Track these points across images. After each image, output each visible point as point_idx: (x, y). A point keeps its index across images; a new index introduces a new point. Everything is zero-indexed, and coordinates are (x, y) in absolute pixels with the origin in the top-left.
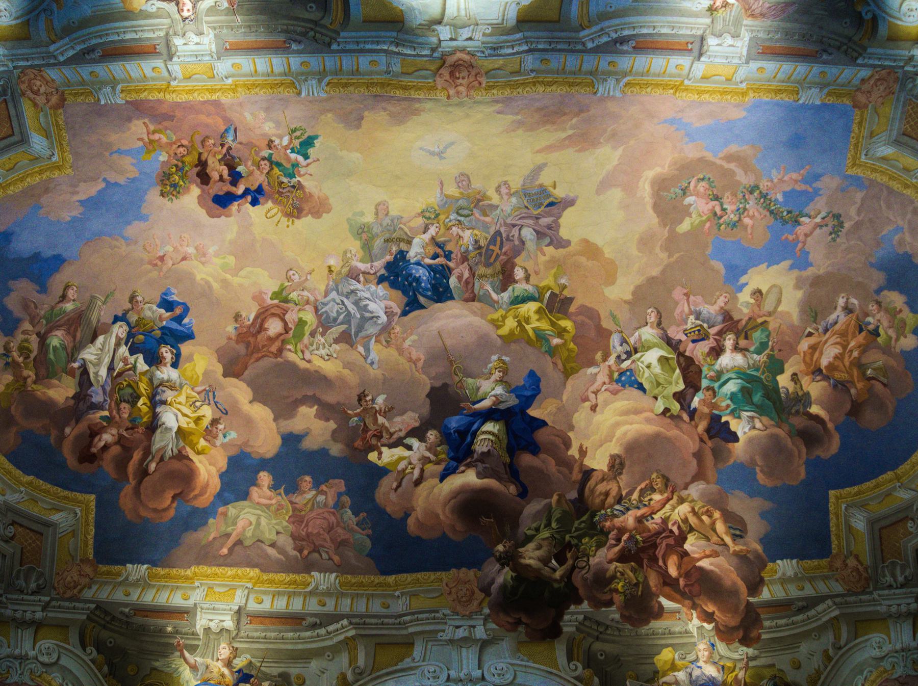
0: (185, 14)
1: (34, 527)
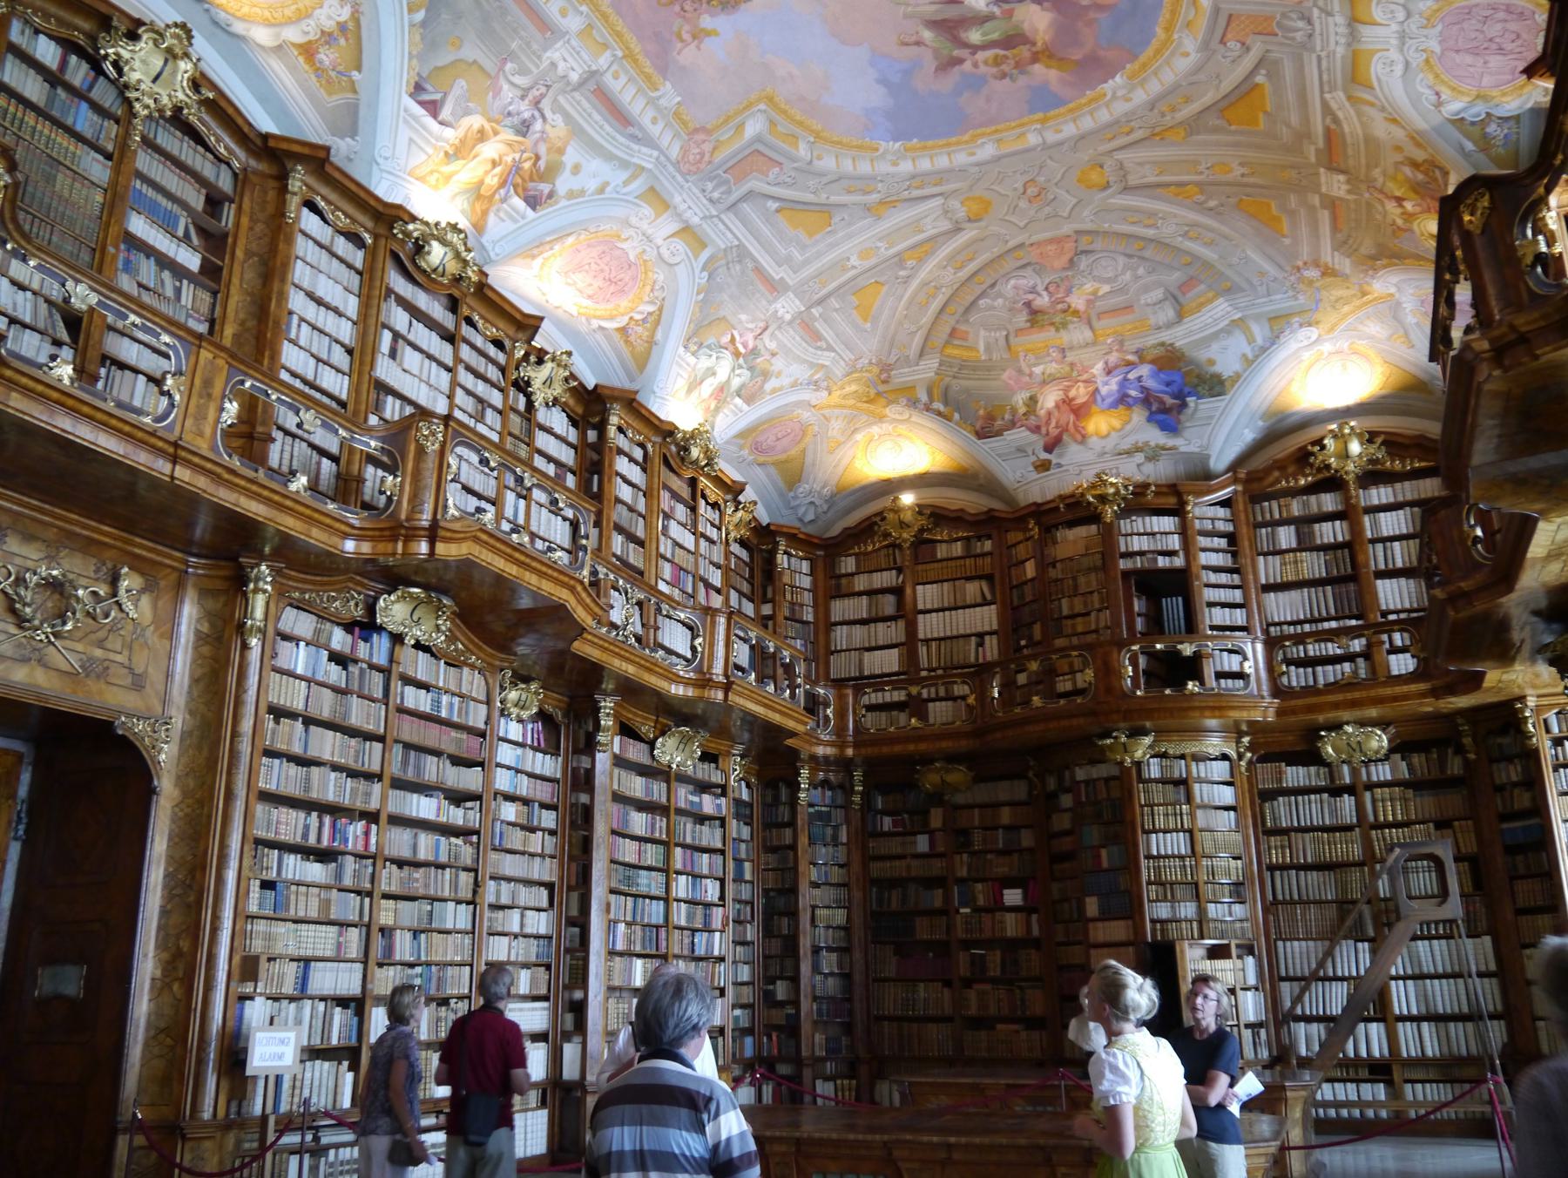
0: (543, 90)
1: (1222, 21)
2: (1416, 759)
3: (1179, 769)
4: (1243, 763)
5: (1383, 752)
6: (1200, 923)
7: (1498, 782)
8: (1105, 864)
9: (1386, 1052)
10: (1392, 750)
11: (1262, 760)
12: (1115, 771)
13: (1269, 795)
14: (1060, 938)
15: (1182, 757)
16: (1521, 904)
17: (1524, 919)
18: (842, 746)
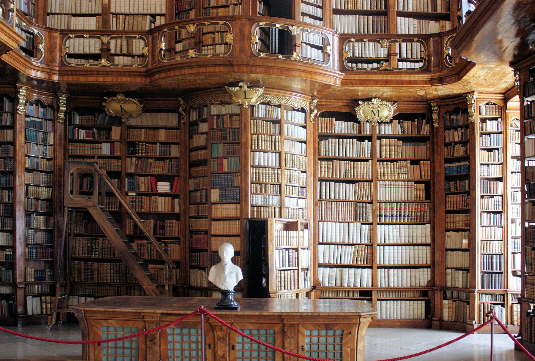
2: (407, 124)
3: (276, 113)
4: (312, 115)
5: (391, 118)
6: (281, 208)
7: (447, 141)
8: (226, 169)
9: (370, 285)
10: (394, 118)
11: (323, 115)
12: (237, 110)
13: (324, 137)
14: (193, 214)
15: (279, 106)
16: (448, 208)
17: (450, 216)
18: (50, 73)
